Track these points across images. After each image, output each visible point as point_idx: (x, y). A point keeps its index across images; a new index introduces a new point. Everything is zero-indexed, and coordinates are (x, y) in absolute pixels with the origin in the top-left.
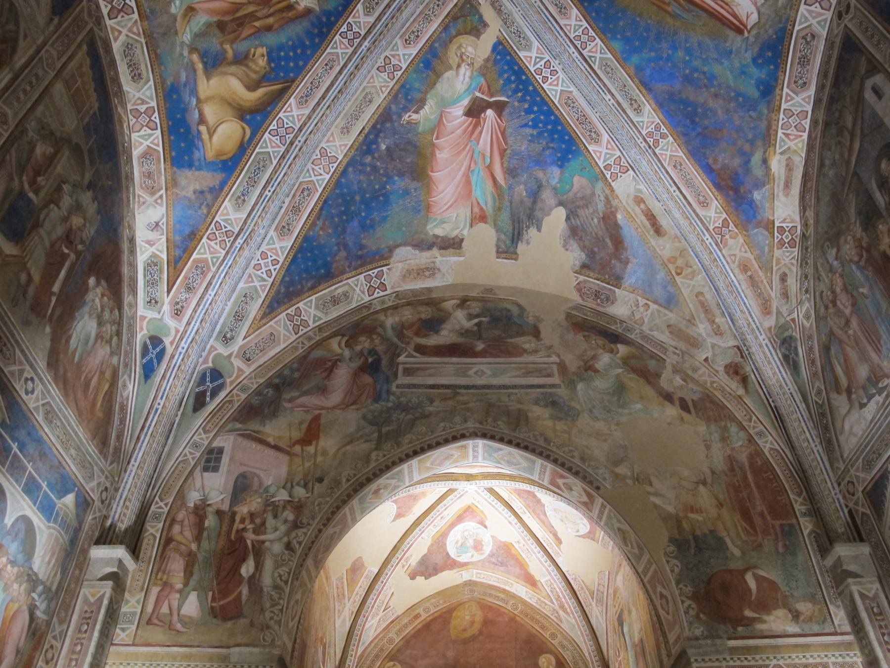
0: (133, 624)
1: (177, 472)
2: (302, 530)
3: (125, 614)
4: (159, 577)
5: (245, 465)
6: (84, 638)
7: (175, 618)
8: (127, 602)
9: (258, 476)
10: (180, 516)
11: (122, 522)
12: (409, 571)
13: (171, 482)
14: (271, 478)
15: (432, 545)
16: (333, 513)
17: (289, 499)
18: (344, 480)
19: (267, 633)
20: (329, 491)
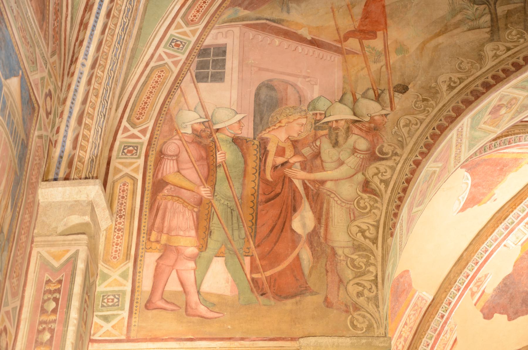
0: (123, 309)
1: (151, 82)
2: (384, 162)
3: (105, 295)
4: (153, 238)
5: (267, 70)
6: (55, 321)
7: (194, 298)
8: (105, 277)
9: (294, 86)
10: (171, 148)
11: (82, 148)
12: (481, 304)
13: (144, 98)
14: (316, 88)
15: (521, 259)
16: (435, 137)
17: (356, 118)
18: (444, 87)
19: (355, 315)
20: (419, 104)
